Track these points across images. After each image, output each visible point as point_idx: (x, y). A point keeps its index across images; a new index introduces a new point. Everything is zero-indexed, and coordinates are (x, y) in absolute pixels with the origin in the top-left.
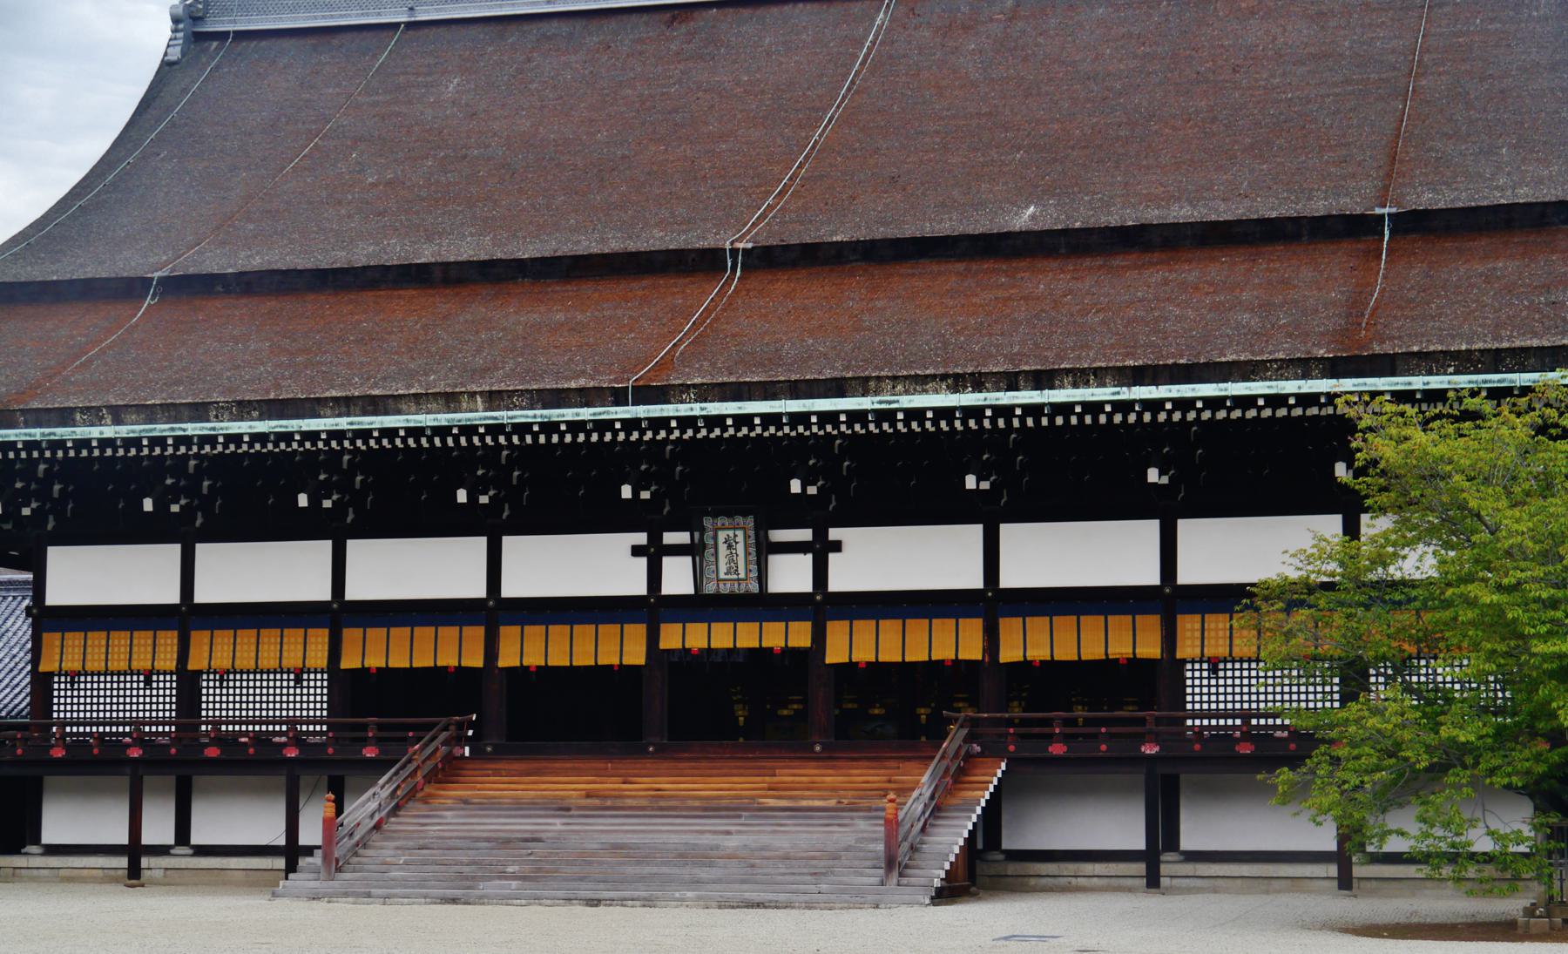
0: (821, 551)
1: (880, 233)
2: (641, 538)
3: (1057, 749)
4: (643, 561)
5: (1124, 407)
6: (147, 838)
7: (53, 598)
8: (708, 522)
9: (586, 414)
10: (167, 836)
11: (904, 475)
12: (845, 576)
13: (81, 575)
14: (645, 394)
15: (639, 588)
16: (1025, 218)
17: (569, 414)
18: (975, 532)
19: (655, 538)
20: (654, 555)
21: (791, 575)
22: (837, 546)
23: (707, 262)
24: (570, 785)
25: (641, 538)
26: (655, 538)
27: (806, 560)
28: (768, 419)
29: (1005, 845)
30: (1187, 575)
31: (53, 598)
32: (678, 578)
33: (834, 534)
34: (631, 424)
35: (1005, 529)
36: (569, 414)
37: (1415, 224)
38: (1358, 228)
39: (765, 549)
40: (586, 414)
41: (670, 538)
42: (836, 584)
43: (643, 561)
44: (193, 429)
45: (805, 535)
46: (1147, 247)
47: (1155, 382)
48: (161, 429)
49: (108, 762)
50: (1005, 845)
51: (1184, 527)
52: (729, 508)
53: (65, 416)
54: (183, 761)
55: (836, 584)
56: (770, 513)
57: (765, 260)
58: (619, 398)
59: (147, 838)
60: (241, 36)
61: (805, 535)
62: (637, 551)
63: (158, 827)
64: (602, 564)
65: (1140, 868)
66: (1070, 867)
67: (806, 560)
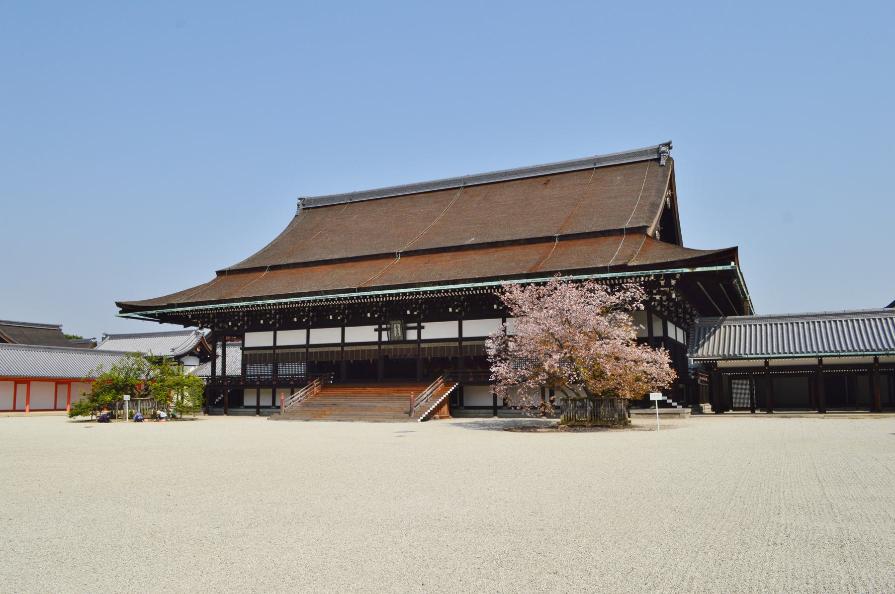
0: (420, 329)
1: (435, 246)
2: (377, 327)
3: (471, 379)
4: (377, 333)
5: (476, 289)
6: (261, 404)
7: (246, 346)
8: (392, 322)
9: (347, 295)
10: (270, 404)
11: (436, 308)
13: (257, 339)
14: (360, 290)
15: (377, 340)
16: (471, 241)
17: (342, 295)
18: (457, 323)
19: (380, 326)
20: (380, 331)
21: (412, 335)
22: (423, 328)
23: (391, 256)
24: (349, 391)
25: (377, 327)
27: (416, 331)
28: (391, 295)
29: (465, 404)
31: (246, 346)
32: (385, 337)
33: (423, 324)
34: (358, 297)
35: (464, 322)
36: (342, 295)
37: (564, 238)
38: (550, 239)
39: (405, 329)
40: (347, 295)
41: (384, 326)
42: (423, 337)
43: (377, 333)
44: (259, 302)
45: (416, 325)
46: (498, 247)
47: (483, 282)
48: (253, 303)
49: (259, 385)
50: (465, 404)
53: (233, 301)
54: (276, 384)
55: (423, 337)
56: (406, 320)
57: (406, 254)
58: (354, 291)
59: (261, 404)
60: (313, 208)
61: (416, 325)
62: (376, 330)
63: (266, 401)
64: (363, 334)
65: (492, 411)
66: (477, 411)
67: (416, 331)
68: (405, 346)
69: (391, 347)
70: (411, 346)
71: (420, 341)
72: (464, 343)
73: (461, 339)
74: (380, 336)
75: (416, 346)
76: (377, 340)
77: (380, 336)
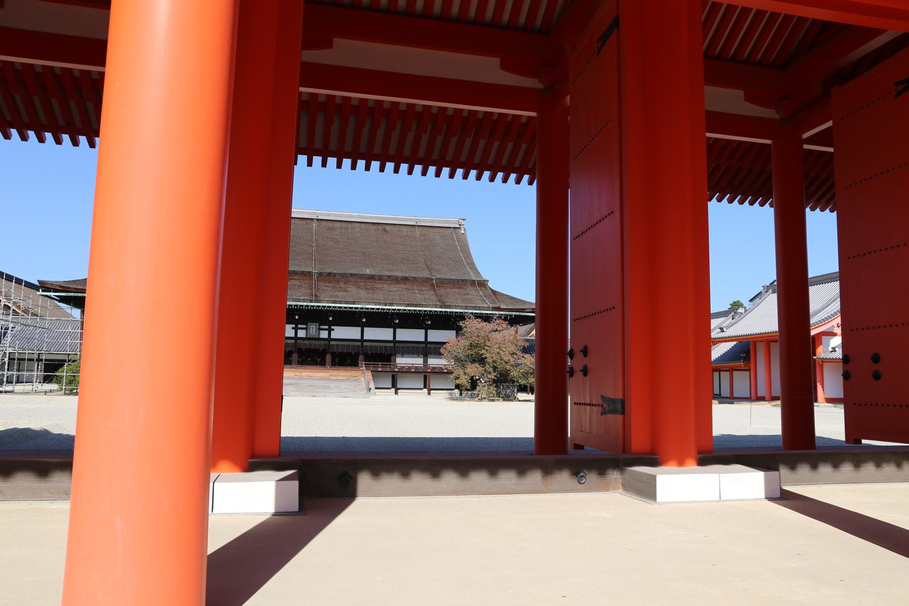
0: (330, 331)
12: (334, 335)
15: (293, 335)
19: (296, 326)
20: (296, 329)
21: (324, 334)
26: (296, 326)
30: (397, 339)
42: (333, 336)
51: (429, 331)
52: (313, 320)
55: (333, 336)
68: (319, 343)
69: (306, 342)
70: (323, 342)
71: (329, 339)
72: (365, 344)
73: (362, 340)
74: (296, 333)
75: (327, 342)
76: (293, 335)
77: (296, 333)
